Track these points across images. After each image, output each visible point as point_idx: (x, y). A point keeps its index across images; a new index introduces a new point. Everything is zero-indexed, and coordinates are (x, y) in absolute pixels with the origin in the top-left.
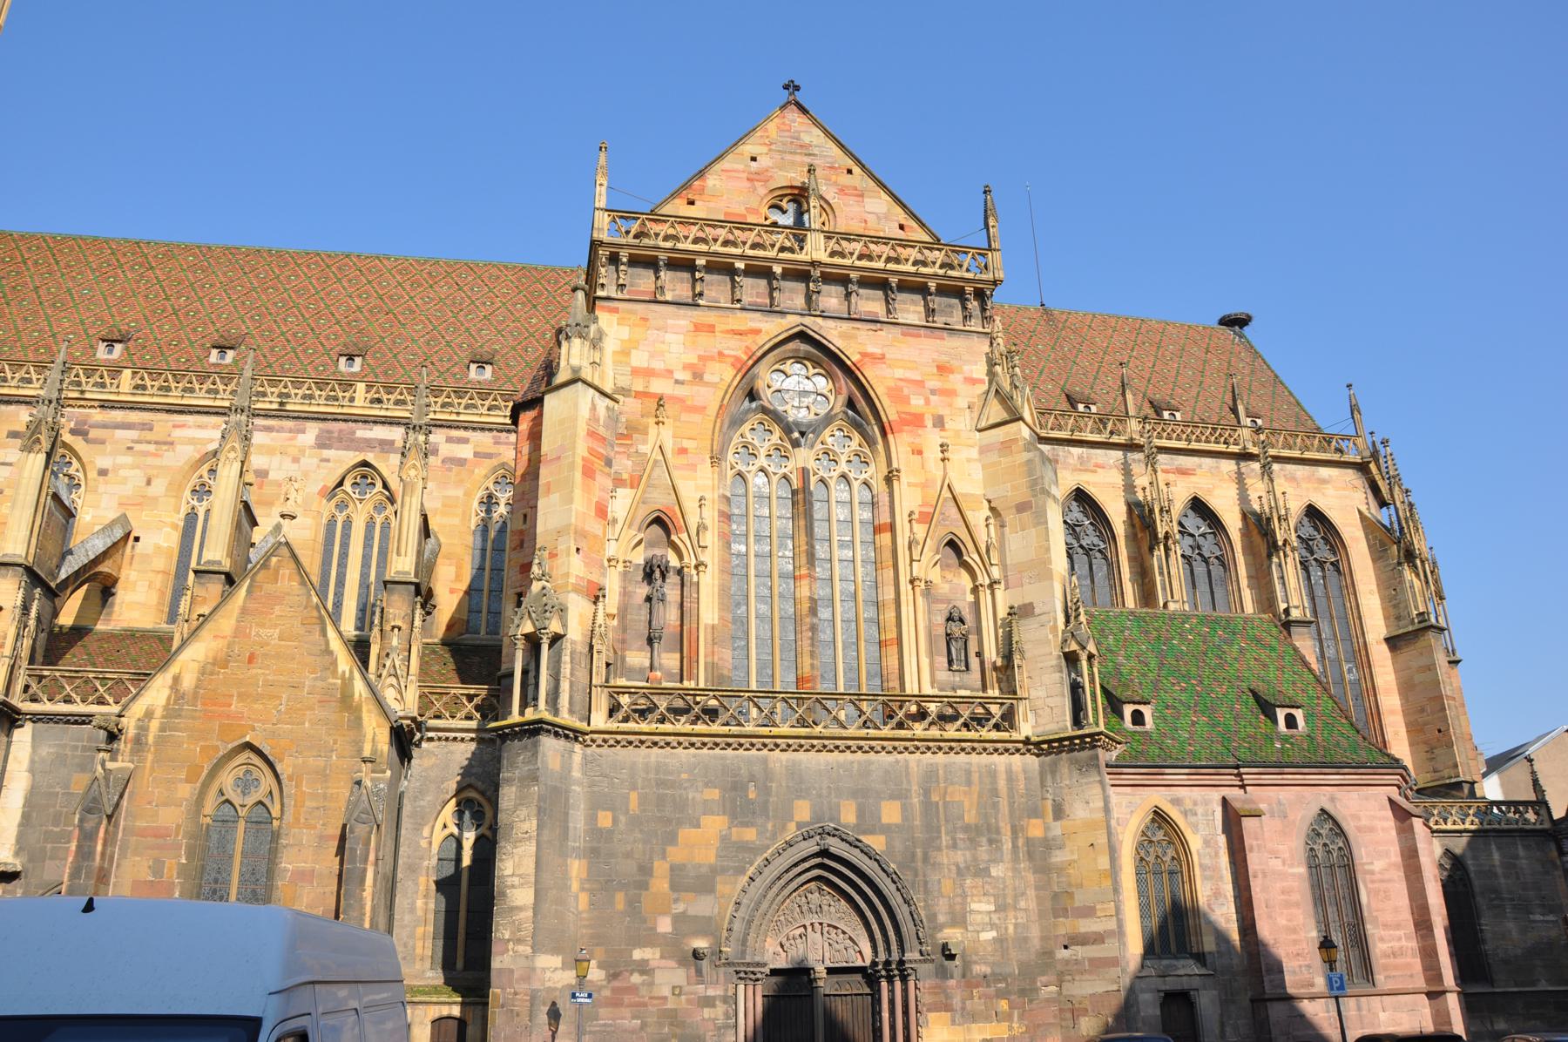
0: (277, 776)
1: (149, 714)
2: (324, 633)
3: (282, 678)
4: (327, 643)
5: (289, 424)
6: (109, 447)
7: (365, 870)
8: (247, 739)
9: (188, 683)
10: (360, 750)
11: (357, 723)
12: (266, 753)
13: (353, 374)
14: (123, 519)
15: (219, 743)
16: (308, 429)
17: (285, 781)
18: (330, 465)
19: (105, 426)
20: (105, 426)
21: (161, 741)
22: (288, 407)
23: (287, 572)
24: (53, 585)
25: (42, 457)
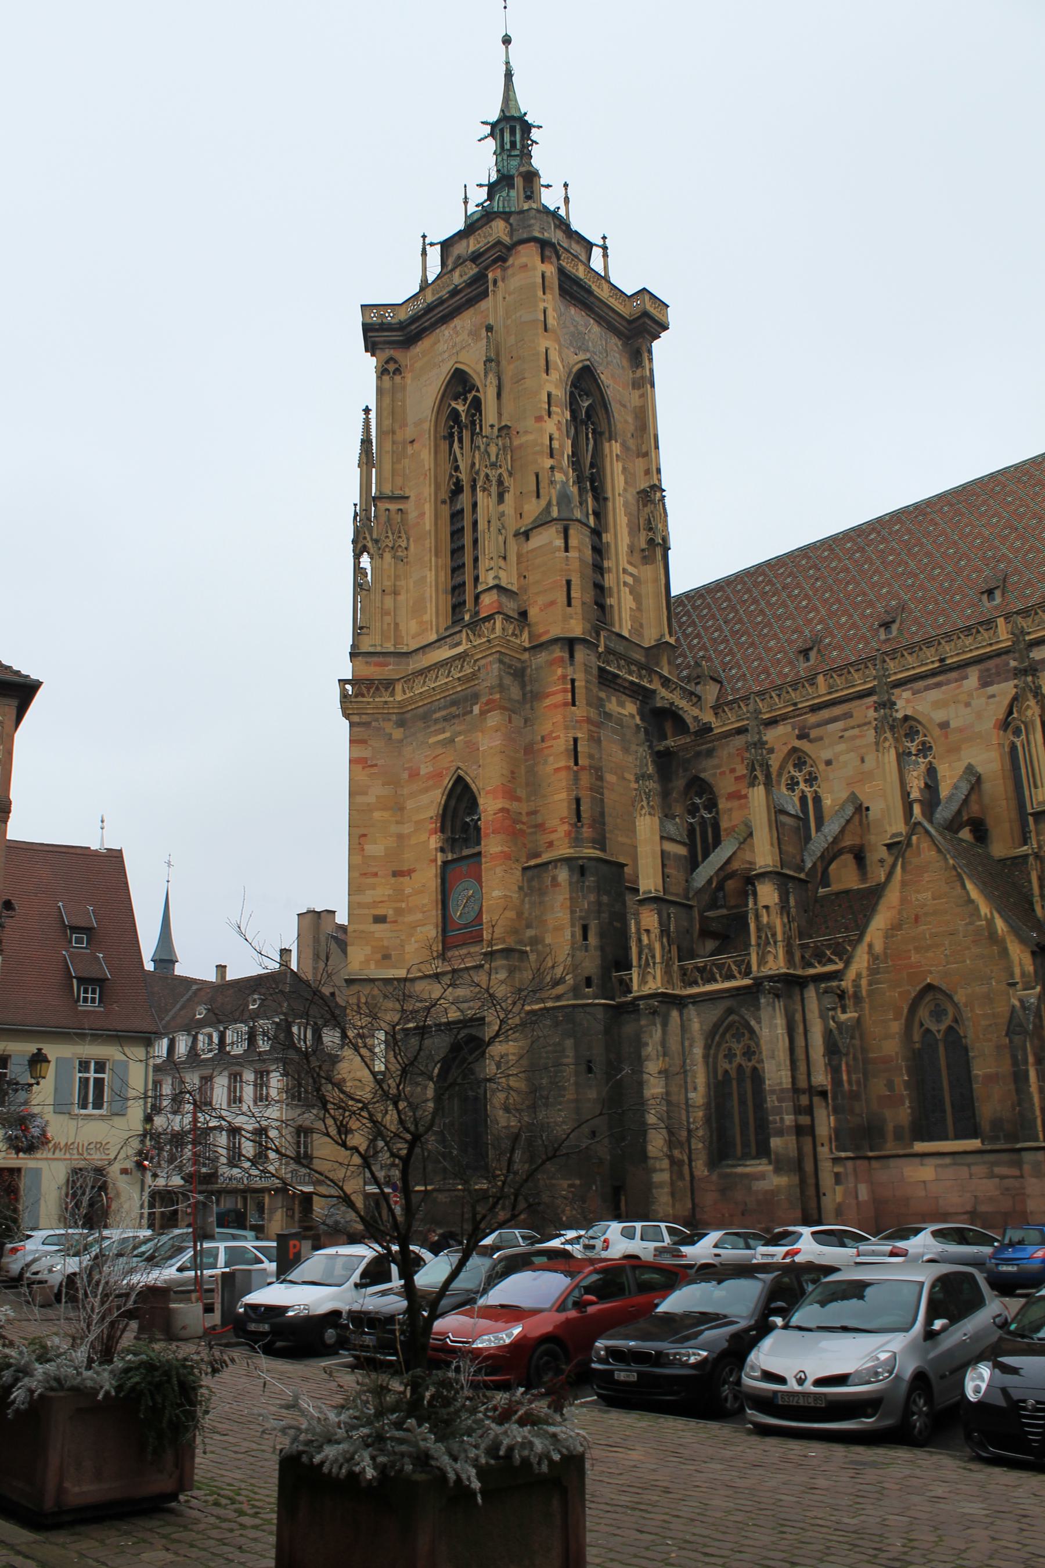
0: (956, 1005)
1: (859, 976)
2: (964, 886)
3: (941, 929)
4: (968, 893)
5: (954, 675)
6: (826, 741)
7: (1027, 1071)
8: (929, 981)
9: (878, 948)
10: (1012, 975)
11: (1004, 952)
12: (944, 988)
13: (996, 608)
14: (853, 798)
15: (909, 988)
16: (970, 674)
17: (963, 1008)
18: (996, 699)
19: (819, 725)
20: (819, 725)
21: (870, 993)
22: (948, 662)
23: (925, 845)
24: (802, 876)
25: (762, 788)
